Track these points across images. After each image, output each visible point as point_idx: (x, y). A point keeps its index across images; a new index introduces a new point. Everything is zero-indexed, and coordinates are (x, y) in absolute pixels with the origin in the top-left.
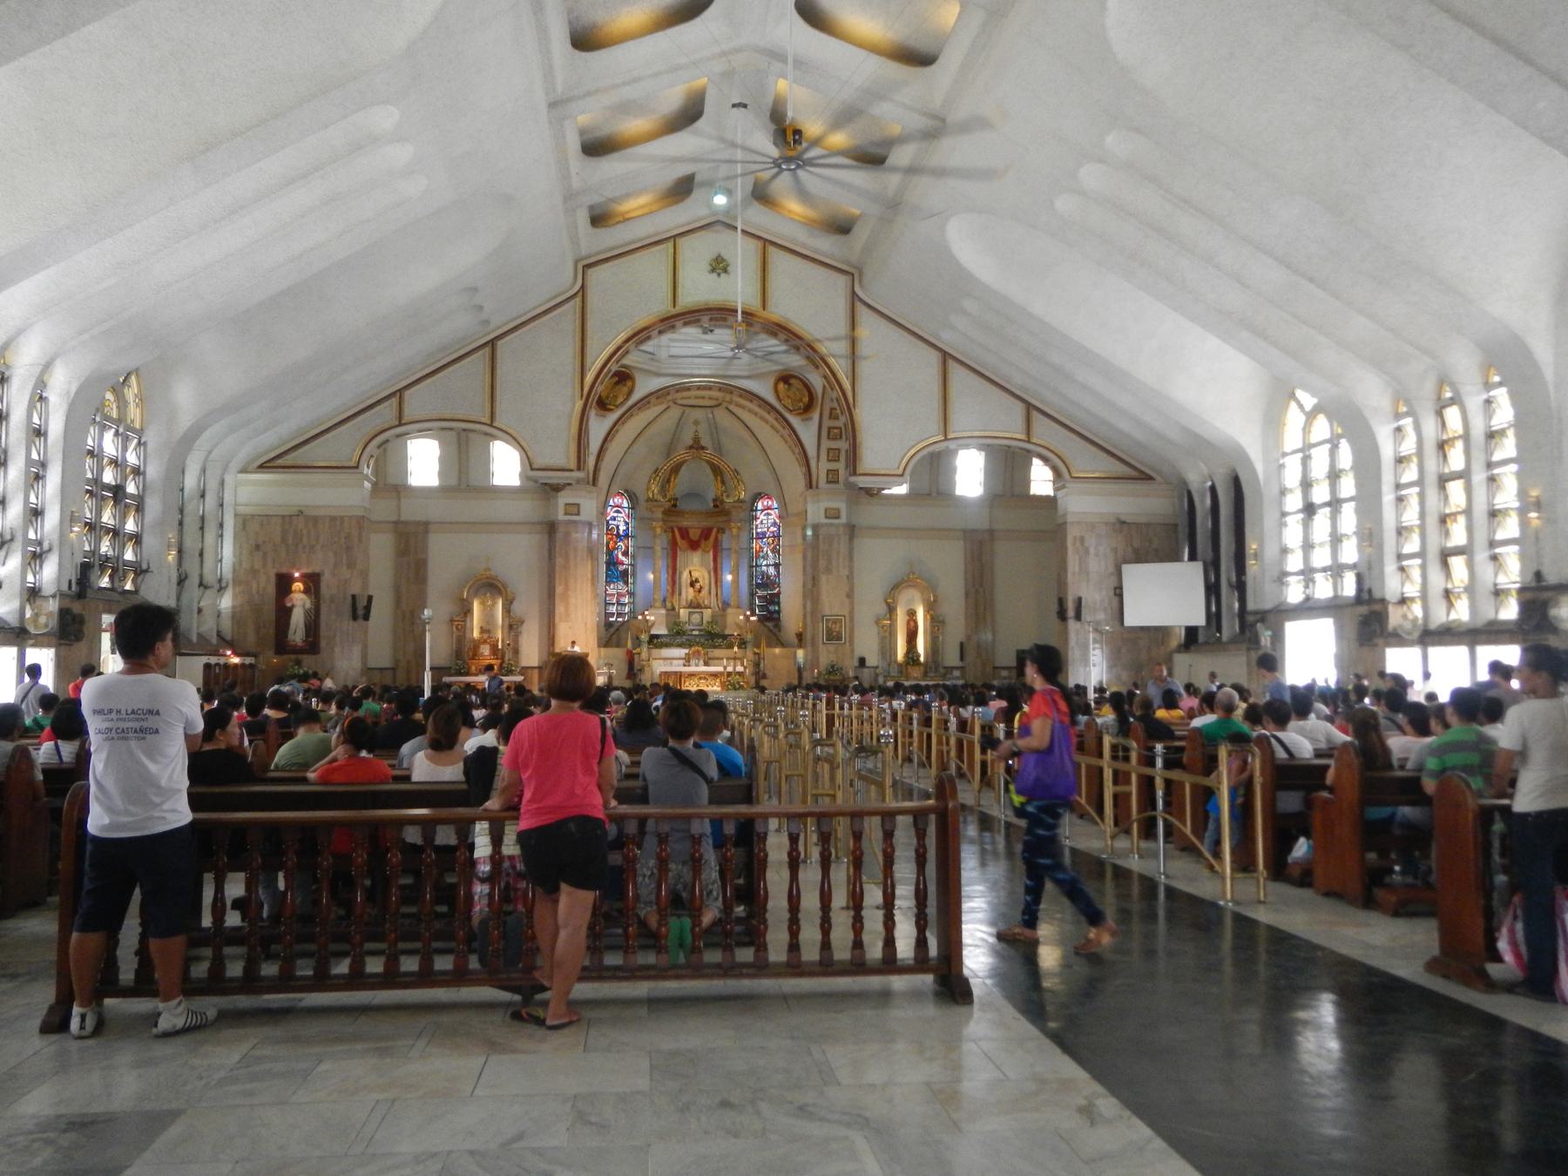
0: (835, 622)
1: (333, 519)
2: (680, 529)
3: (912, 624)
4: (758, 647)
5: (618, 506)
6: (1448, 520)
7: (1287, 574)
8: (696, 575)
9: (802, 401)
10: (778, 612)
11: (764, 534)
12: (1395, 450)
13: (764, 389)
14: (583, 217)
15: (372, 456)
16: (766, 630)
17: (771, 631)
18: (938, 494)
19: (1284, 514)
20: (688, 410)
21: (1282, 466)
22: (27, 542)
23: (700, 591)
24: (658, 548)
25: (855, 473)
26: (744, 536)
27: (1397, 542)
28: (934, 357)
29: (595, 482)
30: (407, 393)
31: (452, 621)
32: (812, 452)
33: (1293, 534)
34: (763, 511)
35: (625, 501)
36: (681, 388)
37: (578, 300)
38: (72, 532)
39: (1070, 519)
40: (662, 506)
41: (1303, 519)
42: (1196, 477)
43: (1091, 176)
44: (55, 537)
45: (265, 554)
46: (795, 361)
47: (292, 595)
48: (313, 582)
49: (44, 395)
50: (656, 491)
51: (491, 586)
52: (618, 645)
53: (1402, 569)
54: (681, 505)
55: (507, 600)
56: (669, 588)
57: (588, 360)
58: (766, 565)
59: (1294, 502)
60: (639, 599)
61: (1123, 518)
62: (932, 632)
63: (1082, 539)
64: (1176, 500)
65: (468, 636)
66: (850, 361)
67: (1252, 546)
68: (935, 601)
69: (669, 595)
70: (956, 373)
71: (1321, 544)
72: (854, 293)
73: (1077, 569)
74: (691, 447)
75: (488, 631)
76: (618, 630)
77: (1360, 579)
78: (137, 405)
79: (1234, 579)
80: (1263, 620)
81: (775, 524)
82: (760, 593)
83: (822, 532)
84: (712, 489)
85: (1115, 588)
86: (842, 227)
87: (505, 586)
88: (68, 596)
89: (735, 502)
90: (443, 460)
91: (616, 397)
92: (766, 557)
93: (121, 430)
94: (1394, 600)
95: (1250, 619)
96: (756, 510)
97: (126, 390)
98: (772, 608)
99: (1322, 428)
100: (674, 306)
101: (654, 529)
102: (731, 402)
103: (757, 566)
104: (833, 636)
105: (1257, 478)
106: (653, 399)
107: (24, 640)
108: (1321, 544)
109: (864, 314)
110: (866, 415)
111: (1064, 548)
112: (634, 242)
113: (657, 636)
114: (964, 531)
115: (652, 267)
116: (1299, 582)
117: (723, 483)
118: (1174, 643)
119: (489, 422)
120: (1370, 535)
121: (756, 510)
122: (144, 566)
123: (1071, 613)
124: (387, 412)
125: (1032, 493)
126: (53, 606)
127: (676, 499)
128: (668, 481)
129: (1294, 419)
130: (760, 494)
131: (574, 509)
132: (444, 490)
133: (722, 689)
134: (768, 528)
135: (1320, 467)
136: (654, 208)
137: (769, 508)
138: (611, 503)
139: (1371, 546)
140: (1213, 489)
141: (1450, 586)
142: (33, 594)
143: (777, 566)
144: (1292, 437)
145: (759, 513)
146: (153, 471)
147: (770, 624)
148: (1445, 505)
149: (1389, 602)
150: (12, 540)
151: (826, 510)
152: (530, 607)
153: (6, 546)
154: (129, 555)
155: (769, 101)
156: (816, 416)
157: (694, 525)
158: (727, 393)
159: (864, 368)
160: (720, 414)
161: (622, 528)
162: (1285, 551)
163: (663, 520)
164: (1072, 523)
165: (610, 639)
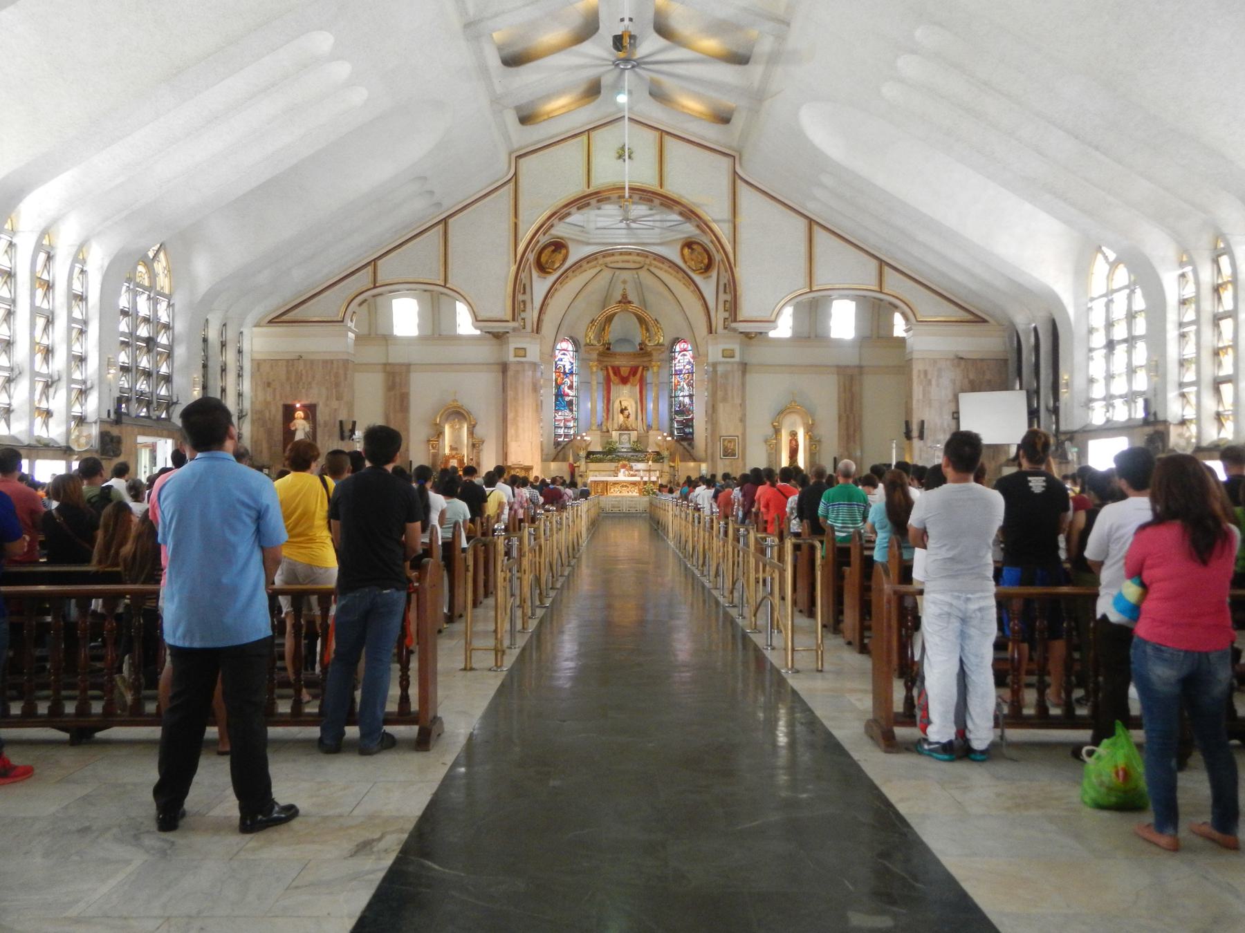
0: (730, 442)
1: (325, 362)
2: (613, 368)
3: (794, 442)
4: (674, 461)
5: (564, 350)
6: (1221, 353)
7: (1092, 400)
8: (624, 404)
9: (702, 262)
10: (692, 434)
11: (681, 371)
12: (1179, 294)
13: (673, 254)
14: (511, 119)
15: (354, 312)
16: (682, 447)
17: (685, 448)
18: (816, 336)
19: (1091, 350)
20: (618, 272)
21: (1090, 309)
22: (71, 381)
23: (628, 417)
24: (594, 383)
25: (735, 320)
26: (665, 372)
27: (1180, 373)
28: (802, 224)
29: (538, 330)
30: (379, 263)
31: (429, 441)
32: (711, 304)
33: (1097, 368)
34: (680, 352)
35: (570, 346)
36: (605, 254)
37: (512, 184)
38: (109, 373)
39: (915, 356)
40: (598, 350)
41: (1105, 354)
42: (1022, 321)
43: (908, 66)
44: (96, 377)
45: (275, 390)
46: (690, 229)
47: (295, 421)
48: (310, 411)
49: (85, 269)
50: (592, 337)
51: (458, 414)
52: (565, 459)
53: (1183, 395)
54: (614, 349)
55: (470, 424)
56: (605, 415)
57: (520, 235)
58: (682, 396)
59: (1099, 340)
60: (582, 423)
61: (961, 355)
62: (810, 450)
63: (926, 373)
64: (1007, 339)
65: (441, 452)
66: (731, 225)
67: (1064, 377)
68: (812, 424)
69: (604, 420)
70: (820, 235)
71: (1120, 375)
72: (735, 172)
73: (921, 397)
74: (620, 302)
75: (456, 449)
76: (563, 448)
77: (1147, 402)
78: (166, 275)
79: (1051, 404)
80: (1071, 439)
81: (689, 363)
82: (678, 418)
83: (720, 369)
84: (638, 335)
85: (953, 413)
86: (723, 118)
87: (469, 413)
88: (107, 422)
89: (656, 345)
90: (421, 315)
91: (553, 262)
92: (682, 390)
93: (152, 295)
94: (1175, 422)
95: (1062, 437)
96: (675, 352)
97: (155, 265)
98: (687, 430)
99: (1122, 276)
100: (589, 187)
101: (591, 368)
102: (650, 265)
103: (675, 397)
104: (728, 453)
105: (1068, 318)
106: (584, 263)
107: (70, 455)
108: (1120, 375)
109: (744, 192)
110: (745, 274)
111: (910, 379)
112: (557, 135)
113: (593, 453)
114: (838, 367)
115: (572, 154)
116: (1102, 407)
117: (647, 330)
118: (1003, 459)
119: (443, 284)
120: (1157, 367)
121: (675, 352)
122: (175, 400)
123: (915, 433)
124: (364, 278)
125: (895, 335)
126: (95, 431)
127: (609, 344)
128: (604, 329)
129: (1100, 267)
130: (678, 339)
131: (520, 352)
132: (423, 339)
133: (640, 494)
134: (684, 366)
135: (1119, 311)
136: (573, 107)
137: (685, 350)
138: (559, 347)
139: (1156, 376)
140: (1035, 329)
141: (1221, 409)
142: (81, 420)
143: (691, 396)
144: (1098, 284)
145: (677, 354)
146: (179, 327)
147: (685, 444)
148: (1218, 340)
149: (1170, 424)
150: (59, 379)
151: (723, 351)
152: (487, 430)
153: (55, 385)
154: (163, 391)
155: (650, 15)
156: (714, 274)
157: (624, 364)
158: (649, 260)
159: (743, 235)
160: (643, 274)
161: (568, 367)
162: (1091, 381)
163: (598, 360)
164: (918, 359)
165: (557, 455)
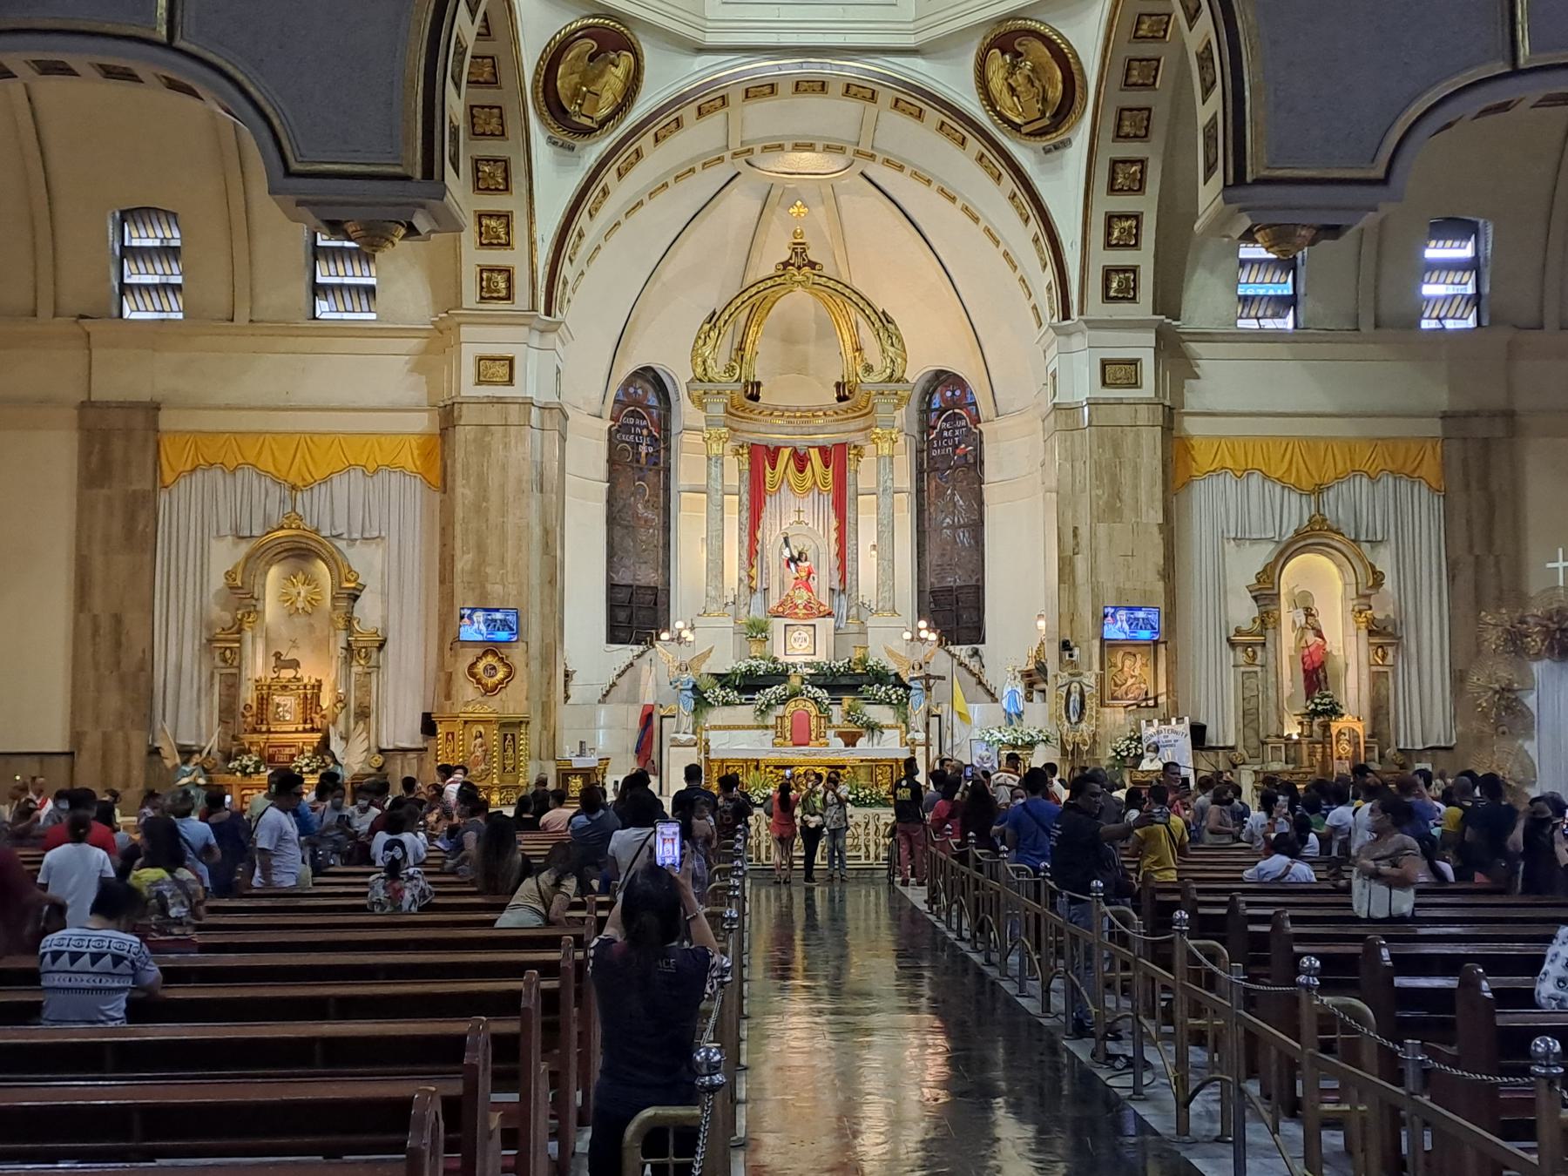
8: (797, 545)
32: (1069, 235)
106: (689, 112)
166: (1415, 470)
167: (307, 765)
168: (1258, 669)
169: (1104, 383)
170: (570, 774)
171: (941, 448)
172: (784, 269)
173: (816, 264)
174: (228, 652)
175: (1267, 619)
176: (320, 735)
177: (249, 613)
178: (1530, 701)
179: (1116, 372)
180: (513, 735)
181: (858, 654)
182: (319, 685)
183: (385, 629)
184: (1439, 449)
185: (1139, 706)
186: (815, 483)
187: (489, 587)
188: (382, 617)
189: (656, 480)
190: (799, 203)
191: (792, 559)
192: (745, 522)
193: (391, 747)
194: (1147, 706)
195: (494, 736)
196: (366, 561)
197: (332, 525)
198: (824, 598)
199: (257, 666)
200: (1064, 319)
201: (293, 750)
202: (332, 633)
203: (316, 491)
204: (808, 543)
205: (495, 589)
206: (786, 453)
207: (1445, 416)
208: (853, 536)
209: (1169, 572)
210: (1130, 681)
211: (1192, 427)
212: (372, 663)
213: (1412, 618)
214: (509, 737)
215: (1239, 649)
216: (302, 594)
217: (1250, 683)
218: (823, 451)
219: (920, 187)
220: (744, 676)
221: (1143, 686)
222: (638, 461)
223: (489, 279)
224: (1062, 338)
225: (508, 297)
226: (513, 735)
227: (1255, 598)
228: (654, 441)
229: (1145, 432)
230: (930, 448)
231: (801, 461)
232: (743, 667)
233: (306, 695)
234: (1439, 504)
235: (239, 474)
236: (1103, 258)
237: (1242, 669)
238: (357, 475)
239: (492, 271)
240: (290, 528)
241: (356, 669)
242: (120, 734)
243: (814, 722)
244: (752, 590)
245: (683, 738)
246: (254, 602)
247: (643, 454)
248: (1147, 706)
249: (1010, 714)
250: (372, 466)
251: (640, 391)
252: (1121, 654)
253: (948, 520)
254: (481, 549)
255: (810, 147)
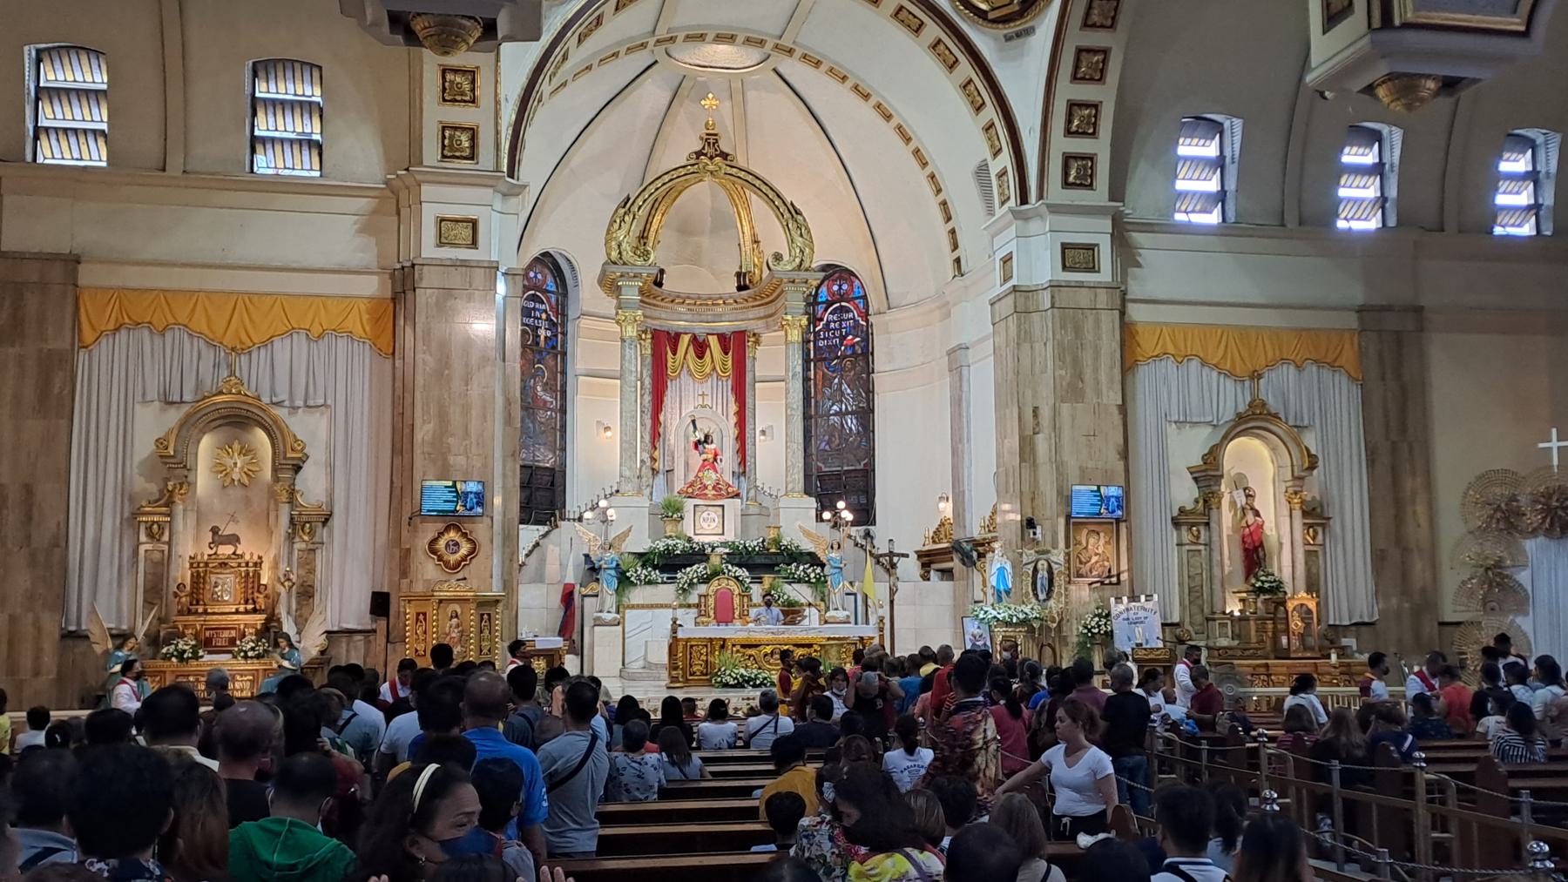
34: (829, 304)
58: (836, 414)
145: (820, 309)
166: (1335, 360)
167: (253, 649)
168: (1202, 547)
169: (1064, 268)
170: (532, 656)
171: (827, 339)
172: (697, 158)
173: (727, 155)
174: (155, 526)
175: (1209, 499)
176: (264, 616)
177: (181, 485)
178: (1523, 577)
179: (1076, 256)
180: (489, 615)
181: (772, 534)
182: (258, 564)
183: (331, 503)
184: (1356, 341)
185: (1102, 583)
186: (714, 369)
187: (451, 459)
188: (327, 490)
189: (553, 363)
190: (710, 96)
191: (697, 444)
192: (647, 405)
193: (335, 629)
194: (1111, 584)
195: (471, 615)
196: (309, 429)
197: (273, 392)
198: (728, 478)
199: (189, 545)
200: (1022, 204)
201: (233, 633)
202: (272, 506)
203: (254, 355)
204: (714, 427)
205: (458, 461)
206: (685, 339)
207: (1361, 310)
208: (751, 420)
209: (1125, 454)
210: (1094, 559)
211: (1137, 313)
212: (317, 539)
213: (1337, 501)
214: (486, 616)
215: (1184, 529)
216: (239, 465)
217: (1196, 561)
218: (722, 338)
219: (832, 84)
220: (661, 555)
221: (1106, 564)
222: (538, 344)
223: (451, 137)
224: (1020, 223)
225: (472, 157)
226: (489, 615)
227: (1196, 479)
228: (552, 326)
229: (1104, 316)
230: (816, 334)
231: (700, 347)
232: (661, 546)
233: (248, 574)
234: (1356, 391)
235: (169, 335)
236: (1061, 145)
237: (1187, 547)
238: (300, 340)
239: (456, 128)
240: (230, 393)
241: (298, 546)
242: (30, 616)
243: (737, 600)
244: (655, 472)
245: (608, 617)
246: (186, 473)
247: (542, 338)
248: (1111, 584)
249: (999, 592)
250: (316, 330)
251: (539, 276)
252: (1085, 532)
253: (835, 407)
254: (443, 417)
255: (730, 39)
